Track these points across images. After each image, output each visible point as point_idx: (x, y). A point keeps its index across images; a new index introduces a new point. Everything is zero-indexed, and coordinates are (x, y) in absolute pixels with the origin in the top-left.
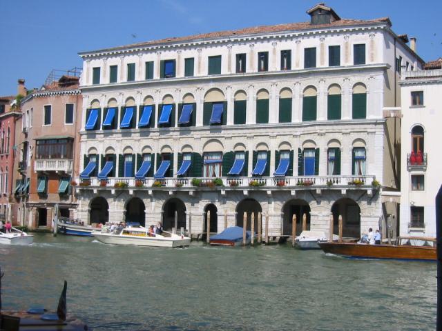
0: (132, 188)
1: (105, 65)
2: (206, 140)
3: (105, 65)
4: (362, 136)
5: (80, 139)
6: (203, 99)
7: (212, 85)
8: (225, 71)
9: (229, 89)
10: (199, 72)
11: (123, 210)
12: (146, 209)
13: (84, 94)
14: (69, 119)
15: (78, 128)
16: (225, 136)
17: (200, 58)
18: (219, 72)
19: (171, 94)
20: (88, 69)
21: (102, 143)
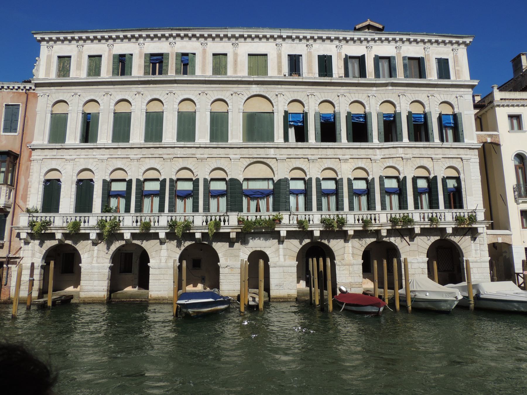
0: (198, 228)
1: (80, 53)
2: (249, 161)
3: (80, 53)
4: (456, 163)
5: (30, 156)
6: (241, 107)
7: (255, 89)
8: (273, 73)
9: (280, 98)
10: (235, 71)
11: (109, 265)
12: (151, 260)
13: (39, 91)
14: (10, 126)
15: (26, 139)
16: (278, 157)
17: (236, 55)
18: (266, 73)
19: (192, 98)
20: (49, 57)
21: (72, 163)
